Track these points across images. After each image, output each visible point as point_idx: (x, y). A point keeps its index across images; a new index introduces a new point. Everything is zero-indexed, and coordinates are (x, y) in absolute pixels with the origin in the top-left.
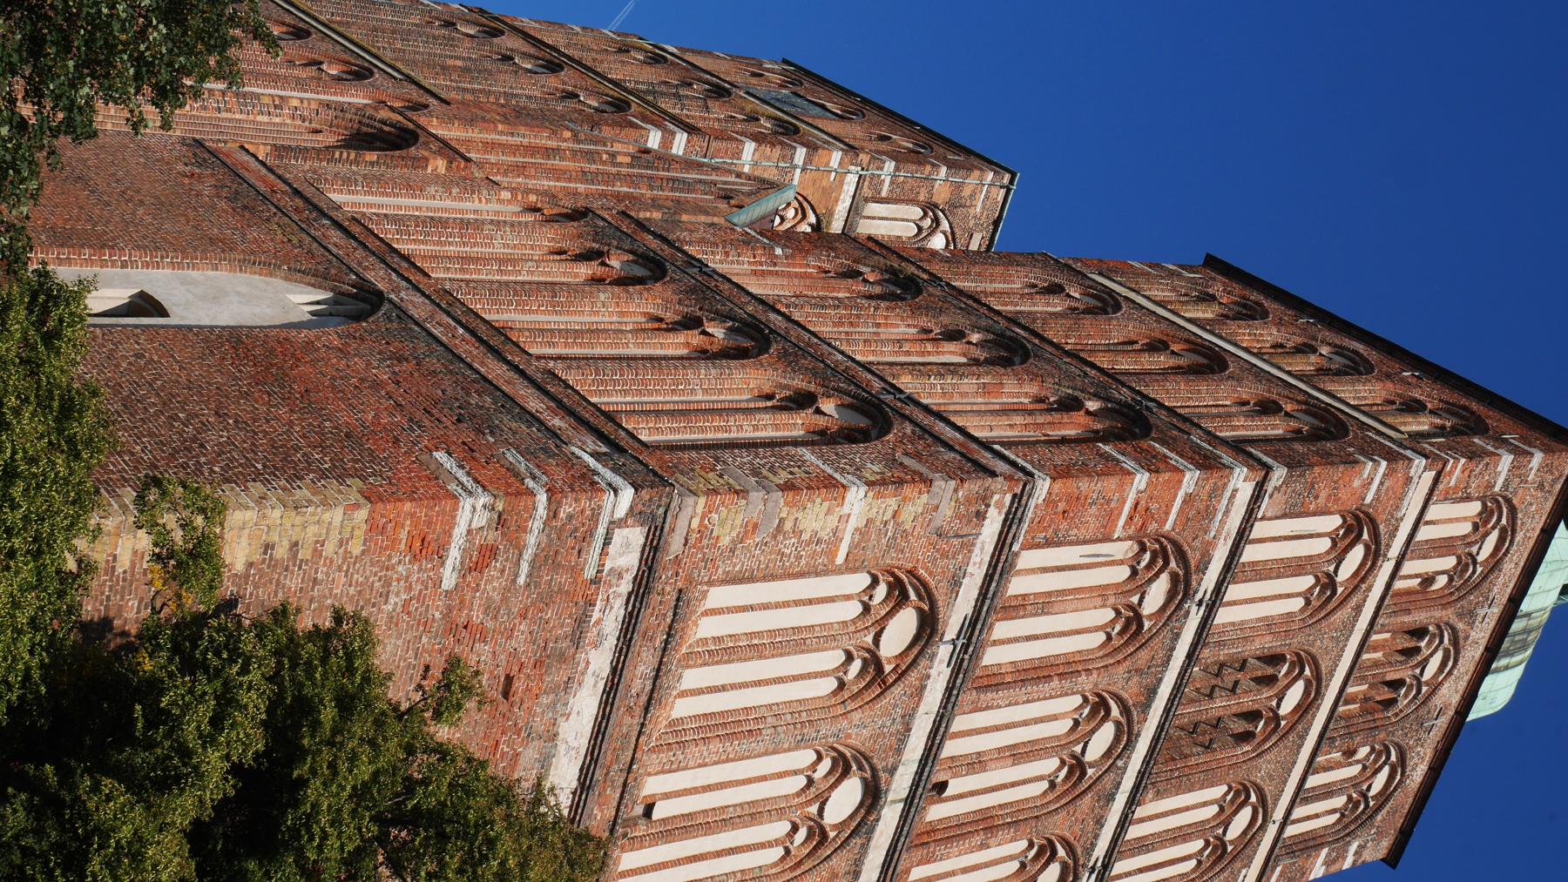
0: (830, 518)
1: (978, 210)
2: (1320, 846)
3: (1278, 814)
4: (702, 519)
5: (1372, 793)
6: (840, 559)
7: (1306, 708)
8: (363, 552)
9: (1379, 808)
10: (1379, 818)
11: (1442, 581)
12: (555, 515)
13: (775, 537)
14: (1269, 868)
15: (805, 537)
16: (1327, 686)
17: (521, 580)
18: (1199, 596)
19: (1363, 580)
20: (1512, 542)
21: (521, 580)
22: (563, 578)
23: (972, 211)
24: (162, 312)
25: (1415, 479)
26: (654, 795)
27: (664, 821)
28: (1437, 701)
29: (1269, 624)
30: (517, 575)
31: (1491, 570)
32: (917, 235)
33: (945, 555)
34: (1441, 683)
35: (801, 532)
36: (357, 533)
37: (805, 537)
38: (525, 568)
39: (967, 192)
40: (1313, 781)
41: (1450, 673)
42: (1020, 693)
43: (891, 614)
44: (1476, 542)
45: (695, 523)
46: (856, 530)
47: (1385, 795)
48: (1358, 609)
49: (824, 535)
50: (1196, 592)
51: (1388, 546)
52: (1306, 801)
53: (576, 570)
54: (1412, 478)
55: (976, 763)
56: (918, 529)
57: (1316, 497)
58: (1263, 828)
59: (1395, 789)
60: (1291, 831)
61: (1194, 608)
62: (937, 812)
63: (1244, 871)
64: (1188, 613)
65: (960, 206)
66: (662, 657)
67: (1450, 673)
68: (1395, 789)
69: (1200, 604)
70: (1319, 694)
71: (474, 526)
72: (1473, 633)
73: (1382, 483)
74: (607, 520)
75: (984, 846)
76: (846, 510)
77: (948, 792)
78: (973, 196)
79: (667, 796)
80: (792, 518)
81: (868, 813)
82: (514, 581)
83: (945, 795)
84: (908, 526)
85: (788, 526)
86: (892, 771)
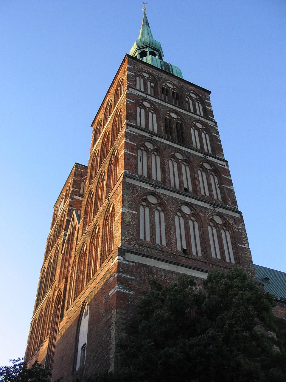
0: (127, 215)
3: (198, 117)
4: (126, 241)
5: (195, 97)
6: (136, 213)
7: (176, 112)
8: (126, 310)
9: (199, 96)
11: (152, 84)
12: (121, 271)
13: (130, 226)
15: (131, 220)
16: (172, 108)
17: (134, 278)
21: (134, 278)
22: (134, 270)
24: (85, 344)
25: (130, 92)
26: (181, 249)
27: (187, 247)
28: (177, 84)
29: (158, 121)
30: (133, 279)
31: (151, 74)
33: (137, 191)
34: (174, 84)
35: (130, 221)
36: (121, 311)
37: (131, 220)
38: (132, 278)
39: (79, 173)
40: (192, 110)
41: (172, 82)
42: (167, 173)
43: (149, 202)
44: (145, 78)
45: (126, 243)
46: (130, 210)
47: (196, 95)
48: (156, 103)
49: (131, 217)
50: (149, 138)
51: (144, 97)
53: (133, 267)
55: (181, 182)
56: (131, 197)
57: (132, 113)
58: (200, 120)
59: (195, 92)
60: (202, 115)
61: (153, 138)
62: (190, 189)
63: (209, 124)
64: (154, 139)
65: (81, 174)
66: (152, 248)
69: (152, 137)
70: (174, 110)
71: (122, 288)
72: (164, 78)
73: (131, 99)
74: (123, 261)
75: (199, 180)
76: (126, 212)
77: (187, 188)
78: (80, 172)
79: (182, 246)
80: (127, 223)
81: (189, 204)
82: (134, 280)
83: (187, 188)
84: (130, 199)
85: (128, 224)
86: (180, 200)
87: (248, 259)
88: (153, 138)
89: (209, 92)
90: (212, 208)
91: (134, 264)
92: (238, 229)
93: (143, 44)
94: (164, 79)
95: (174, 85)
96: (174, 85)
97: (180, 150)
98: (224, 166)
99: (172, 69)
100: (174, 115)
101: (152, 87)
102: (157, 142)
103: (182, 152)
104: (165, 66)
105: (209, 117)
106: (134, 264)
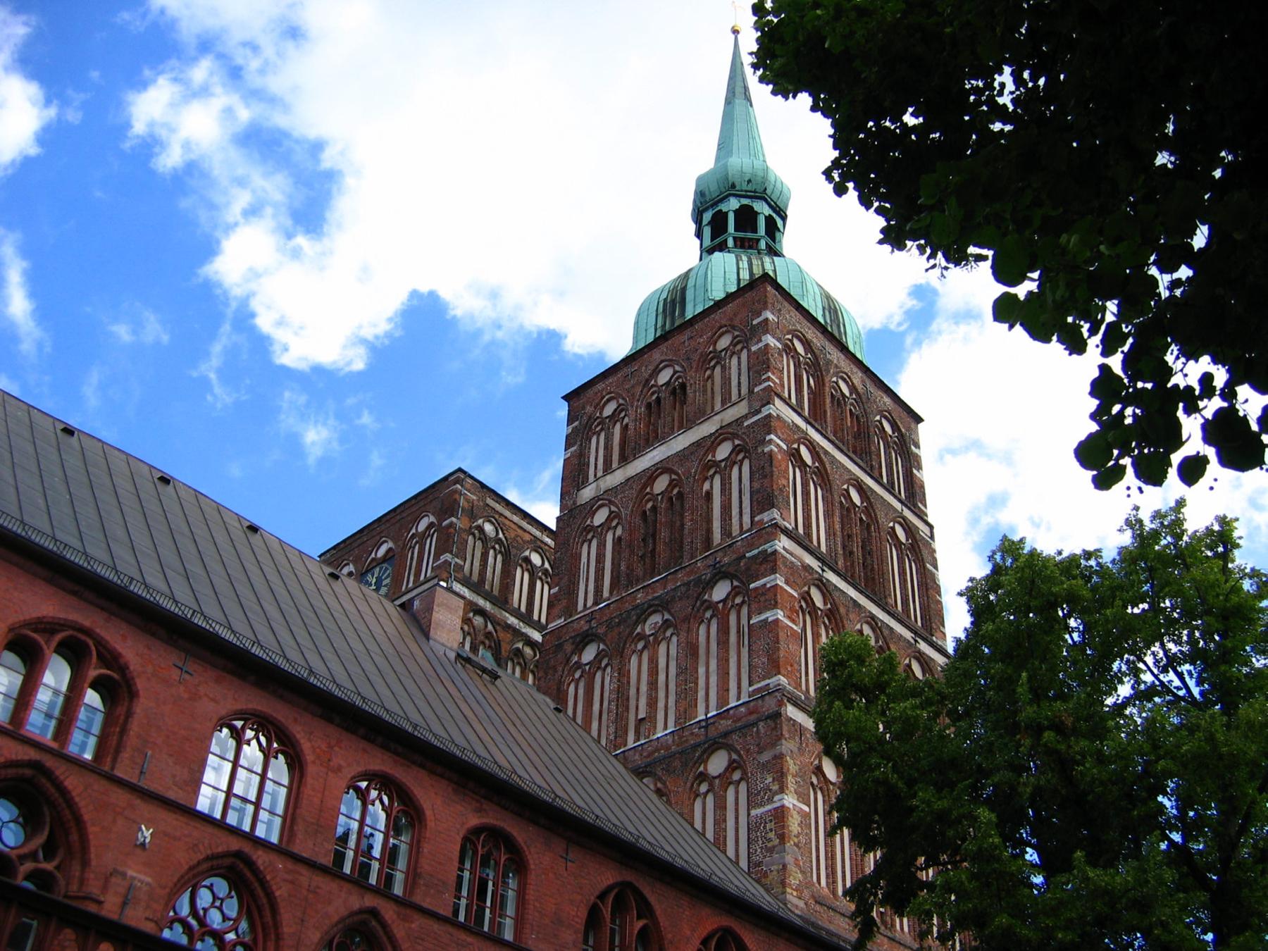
1: (475, 498)
2: (912, 472)
7: (861, 489)
9: (899, 430)
14: (916, 511)
19: (814, 448)
20: (801, 333)
23: (476, 503)
28: (860, 387)
32: (482, 542)
34: (853, 383)
39: (466, 505)
48: (826, 452)
52: (893, 488)
58: (904, 518)
65: (472, 510)
67: (849, 377)
68: (892, 417)
88: (825, 574)
89: (919, 420)
93: (749, 181)
95: (853, 388)
96: (853, 388)
97: (873, 617)
99: (844, 325)
102: (833, 590)
103: (877, 624)
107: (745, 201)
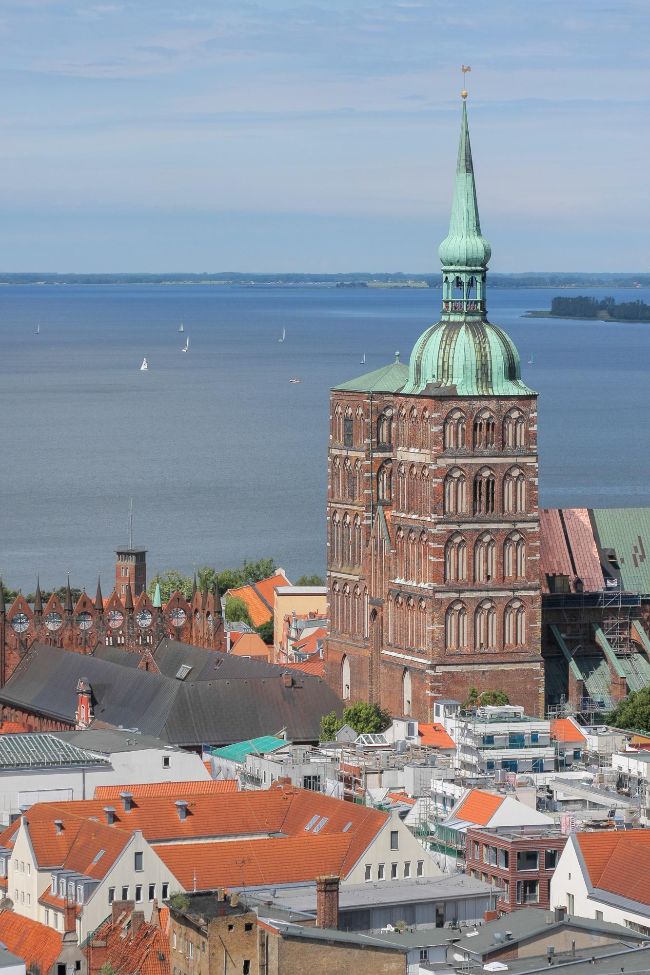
10: (524, 410)
18: (457, 528)
25: (438, 465)
29: (467, 493)
47: (519, 409)
54: (438, 467)
63: (527, 464)
86: (481, 597)
87: (537, 638)
90: (510, 594)
91: (441, 674)
92: (533, 608)
93: (458, 261)
94: (479, 408)
98: (534, 528)
99: (491, 370)
100: (486, 473)
101: (463, 429)
104: (481, 369)
105: (531, 447)
106: (441, 674)
107: (457, 274)
